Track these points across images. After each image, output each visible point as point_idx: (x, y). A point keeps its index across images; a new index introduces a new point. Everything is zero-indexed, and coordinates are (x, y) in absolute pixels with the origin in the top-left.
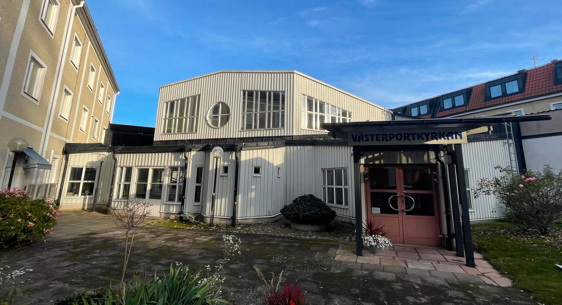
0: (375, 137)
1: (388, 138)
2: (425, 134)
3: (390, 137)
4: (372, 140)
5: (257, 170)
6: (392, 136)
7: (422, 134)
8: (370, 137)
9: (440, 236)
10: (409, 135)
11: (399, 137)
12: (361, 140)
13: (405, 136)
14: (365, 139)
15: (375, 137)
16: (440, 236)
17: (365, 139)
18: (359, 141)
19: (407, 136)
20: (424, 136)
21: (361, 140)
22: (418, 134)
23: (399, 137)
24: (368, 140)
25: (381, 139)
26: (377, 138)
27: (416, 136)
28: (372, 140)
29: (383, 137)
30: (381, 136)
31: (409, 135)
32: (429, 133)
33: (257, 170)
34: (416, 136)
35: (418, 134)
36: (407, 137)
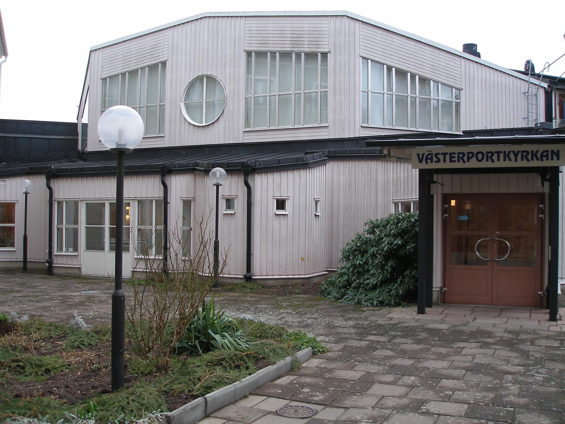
0: (448, 157)
1: (465, 158)
2: (514, 152)
3: (468, 156)
4: (445, 161)
5: (281, 204)
6: (471, 155)
7: (510, 152)
8: (441, 157)
9: (540, 293)
10: (493, 154)
11: (480, 156)
12: (429, 161)
13: (487, 156)
14: (435, 159)
15: (448, 157)
16: (540, 293)
17: (435, 159)
18: (427, 163)
19: (490, 155)
20: (512, 156)
21: (429, 161)
22: (505, 152)
23: (480, 156)
24: (439, 161)
25: (456, 159)
26: (451, 157)
27: (502, 155)
28: (445, 161)
29: (459, 156)
30: (456, 156)
31: (493, 154)
32: (518, 152)
33: (281, 204)
34: (502, 155)
35: (505, 152)
36: (489, 156)
